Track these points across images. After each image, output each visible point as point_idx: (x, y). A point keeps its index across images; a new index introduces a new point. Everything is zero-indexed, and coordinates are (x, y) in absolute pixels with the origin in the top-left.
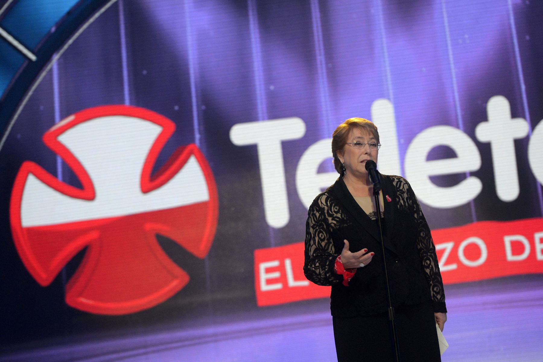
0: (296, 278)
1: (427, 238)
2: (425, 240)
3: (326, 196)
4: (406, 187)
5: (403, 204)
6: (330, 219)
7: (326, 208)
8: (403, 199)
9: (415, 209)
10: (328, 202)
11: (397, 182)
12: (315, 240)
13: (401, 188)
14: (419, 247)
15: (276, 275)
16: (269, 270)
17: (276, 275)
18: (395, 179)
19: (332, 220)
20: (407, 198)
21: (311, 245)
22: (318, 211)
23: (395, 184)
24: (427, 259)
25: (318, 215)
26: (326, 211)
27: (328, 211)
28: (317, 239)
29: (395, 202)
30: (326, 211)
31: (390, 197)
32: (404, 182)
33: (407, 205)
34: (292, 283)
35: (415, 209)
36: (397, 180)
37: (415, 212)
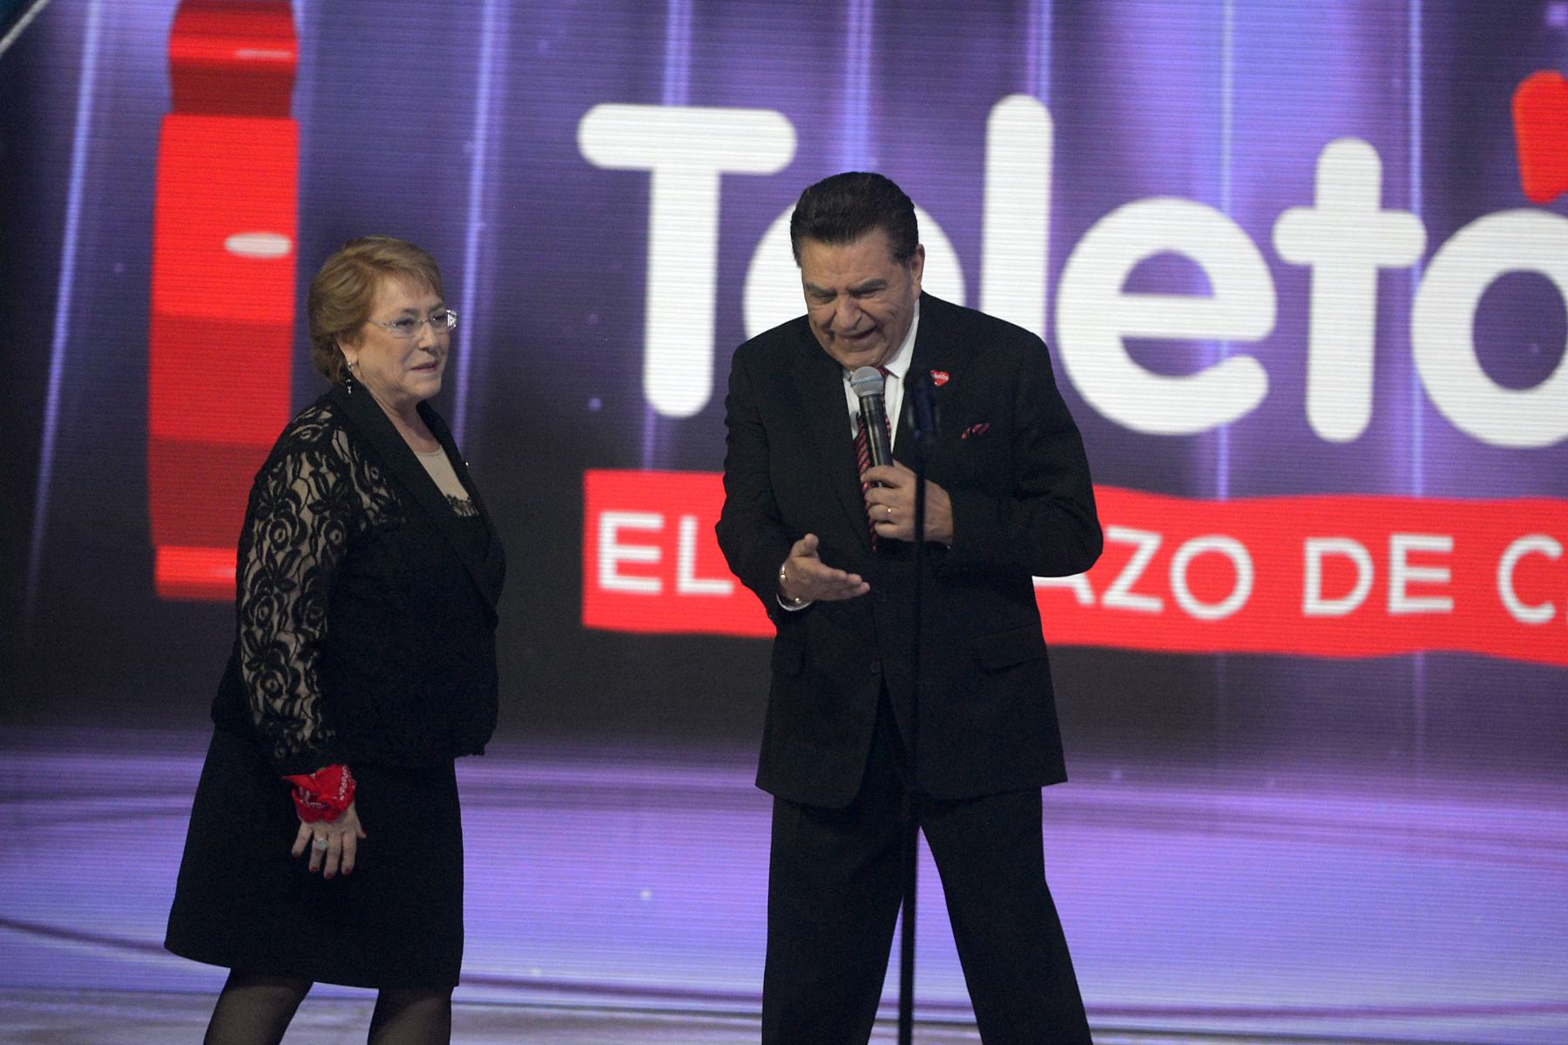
0: (701, 571)
12: (316, 543)
15: (650, 554)
16: (626, 536)
17: (650, 554)
21: (251, 561)
34: (688, 583)
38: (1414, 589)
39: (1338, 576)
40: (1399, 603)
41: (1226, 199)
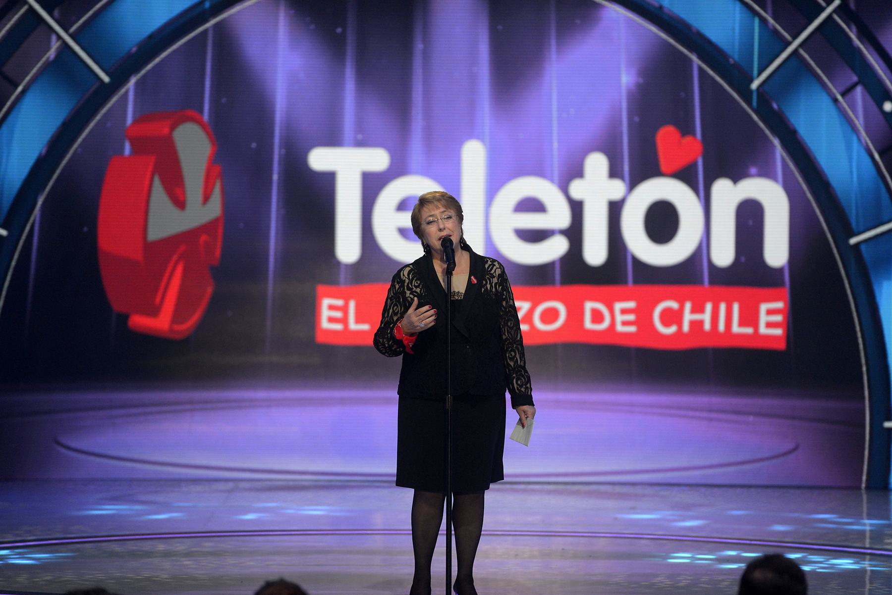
1: (515, 328)
2: (513, 331)
3: (410, 268)
4: (499, 272)
5: (489, 288)
6: (408, 292)
7: (407, 281)
8: (491, 284)
9: (504, 297)
10: (411, 275)
11: (490, 265)
13: (493, 271)
14: (504, 337)
18: (489, 261)
19: (410, 294)
20: (496, 284)
22: (398, 283)
23: (487, 266)
24: (511, 351)
25: (397, 287)
26: (406, 284)
27: (408, 284)
28: (391, 311)
29: (480, 285)
30: (406, 284)
31: (475, 278)
32: (497, 266)
33: (494, 290)
35: (504, 297)
36: (491, 263)
37: (504, 300)
38: (625, 323)
39: (597, 317)
40: (620, 328)
41: (556, 178)
